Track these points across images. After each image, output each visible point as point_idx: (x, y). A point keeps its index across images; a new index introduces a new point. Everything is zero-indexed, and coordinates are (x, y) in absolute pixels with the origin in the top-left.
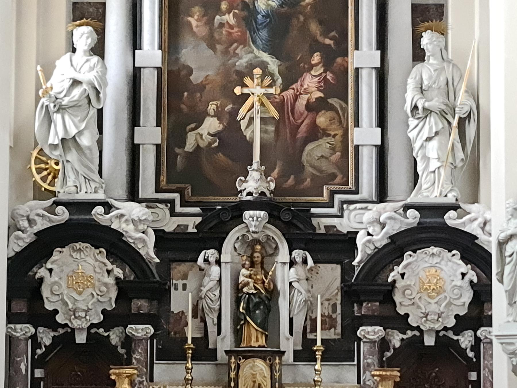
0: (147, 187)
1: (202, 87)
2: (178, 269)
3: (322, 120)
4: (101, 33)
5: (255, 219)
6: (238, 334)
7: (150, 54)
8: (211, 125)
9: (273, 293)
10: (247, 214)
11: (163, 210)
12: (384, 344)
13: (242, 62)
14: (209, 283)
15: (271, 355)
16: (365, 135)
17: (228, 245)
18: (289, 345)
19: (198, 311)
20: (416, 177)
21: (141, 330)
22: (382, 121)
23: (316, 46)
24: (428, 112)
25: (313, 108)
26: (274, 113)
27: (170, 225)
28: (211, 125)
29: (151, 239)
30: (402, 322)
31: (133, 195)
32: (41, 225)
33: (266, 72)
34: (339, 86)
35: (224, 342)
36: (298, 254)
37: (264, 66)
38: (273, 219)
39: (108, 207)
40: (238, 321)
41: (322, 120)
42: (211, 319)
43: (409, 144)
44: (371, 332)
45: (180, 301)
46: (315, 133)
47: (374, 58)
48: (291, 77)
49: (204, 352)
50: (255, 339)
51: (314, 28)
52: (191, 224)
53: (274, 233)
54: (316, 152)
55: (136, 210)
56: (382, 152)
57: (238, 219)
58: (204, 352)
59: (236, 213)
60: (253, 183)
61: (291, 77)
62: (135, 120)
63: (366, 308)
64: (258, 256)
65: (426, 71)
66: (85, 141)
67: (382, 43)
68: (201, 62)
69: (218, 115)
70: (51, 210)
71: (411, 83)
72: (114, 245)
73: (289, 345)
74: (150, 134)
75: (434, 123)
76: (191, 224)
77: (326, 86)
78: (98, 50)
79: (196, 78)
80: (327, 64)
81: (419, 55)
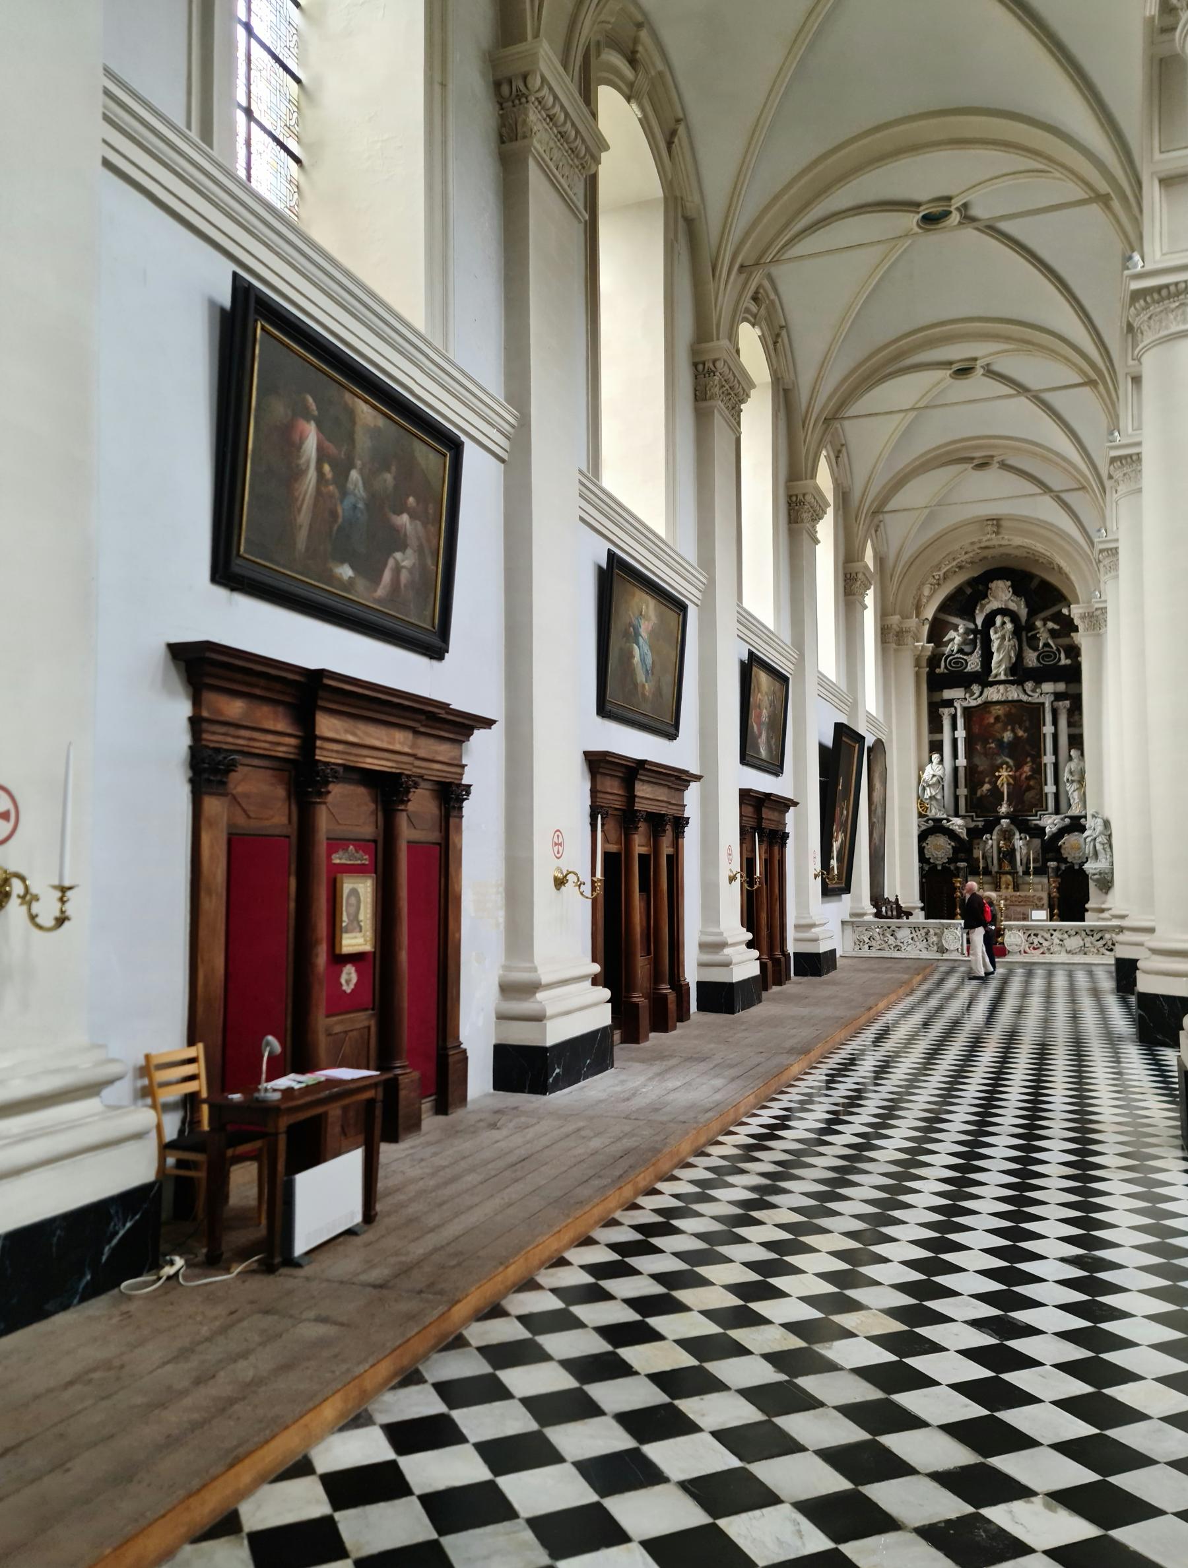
0: (962, 811)
1: (982, 772)
2: (976, 841)
3: (1032, 783)
4: (942, 756)
5: (1005, 822)
6: (1000, 866)
7: (962, 761)
8: (987, 787)
9: (1013, 850)
10: (1003, 821)
11: (969, 820)
12: (1058, 869)
13: (999, 761)
14: (988, 847)
15: (1014, 873)
16: (1050, 789)
17: (995, 832)
18: (1020, 869)
19: (984, 857)
20: (1070, 805)
21: (962, 865)
22: (1057, 782)
23: (1029, 755)
24: (1073, 781)
25: (1028, 778)
26: (1011, 781)
27: (972, 825)
28: (987, 787)
29: (965, 831)
30: (1065, 860)
31: (957, 815)
32: (923, 828)
33: (1008, 766)
34: (1039, 769)
35: (995, 869)
36: (1023, 835)
37: (1007, 763)
38: (1012, 822)
39: (948, 821)
40: (1000, 860)
41: (1032, 783)
42: (989, 860)
43: (1067, 793)
44: (1052, 864)
45: (978, 853)
46: (1029, 788)
47: (1053, 759)
48: (1019, 766)
49: (987, 872)
50: (1007, 868)
51: (1028, 748)
52: (981, 824)
53: (1012, 827)
54: (1029, 795)
55: (959, 821)
56: (1057, 795)
57: (999, 823)
58: (987, 872)
59: (997, 821)
60: (1004, 809)
61: (1019, 766)
62: (956, 786)
63: (1050, 855)
64: (1007, 836)
65: (1073, 765)
66: (938, 797)
67: (1056, 752)
68: (982, 764)
69: (989, 782)
70: (927, 822)
71: (1067, 770)
72: (951, 834)
73: (1020, 869)
74: (963, 791)
75: (1075, 786)
76: (981, 824)
77: (1032, 769)
78: (941, 761)
79: (981, 768)
80: (1033, 761)
81: (1070, 758)
